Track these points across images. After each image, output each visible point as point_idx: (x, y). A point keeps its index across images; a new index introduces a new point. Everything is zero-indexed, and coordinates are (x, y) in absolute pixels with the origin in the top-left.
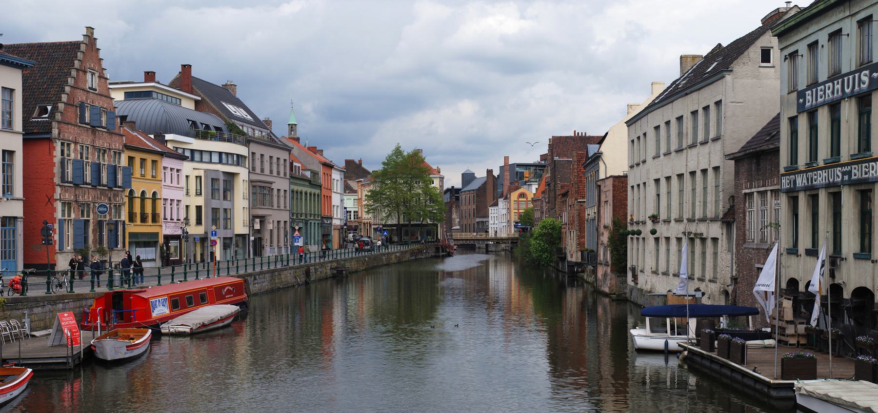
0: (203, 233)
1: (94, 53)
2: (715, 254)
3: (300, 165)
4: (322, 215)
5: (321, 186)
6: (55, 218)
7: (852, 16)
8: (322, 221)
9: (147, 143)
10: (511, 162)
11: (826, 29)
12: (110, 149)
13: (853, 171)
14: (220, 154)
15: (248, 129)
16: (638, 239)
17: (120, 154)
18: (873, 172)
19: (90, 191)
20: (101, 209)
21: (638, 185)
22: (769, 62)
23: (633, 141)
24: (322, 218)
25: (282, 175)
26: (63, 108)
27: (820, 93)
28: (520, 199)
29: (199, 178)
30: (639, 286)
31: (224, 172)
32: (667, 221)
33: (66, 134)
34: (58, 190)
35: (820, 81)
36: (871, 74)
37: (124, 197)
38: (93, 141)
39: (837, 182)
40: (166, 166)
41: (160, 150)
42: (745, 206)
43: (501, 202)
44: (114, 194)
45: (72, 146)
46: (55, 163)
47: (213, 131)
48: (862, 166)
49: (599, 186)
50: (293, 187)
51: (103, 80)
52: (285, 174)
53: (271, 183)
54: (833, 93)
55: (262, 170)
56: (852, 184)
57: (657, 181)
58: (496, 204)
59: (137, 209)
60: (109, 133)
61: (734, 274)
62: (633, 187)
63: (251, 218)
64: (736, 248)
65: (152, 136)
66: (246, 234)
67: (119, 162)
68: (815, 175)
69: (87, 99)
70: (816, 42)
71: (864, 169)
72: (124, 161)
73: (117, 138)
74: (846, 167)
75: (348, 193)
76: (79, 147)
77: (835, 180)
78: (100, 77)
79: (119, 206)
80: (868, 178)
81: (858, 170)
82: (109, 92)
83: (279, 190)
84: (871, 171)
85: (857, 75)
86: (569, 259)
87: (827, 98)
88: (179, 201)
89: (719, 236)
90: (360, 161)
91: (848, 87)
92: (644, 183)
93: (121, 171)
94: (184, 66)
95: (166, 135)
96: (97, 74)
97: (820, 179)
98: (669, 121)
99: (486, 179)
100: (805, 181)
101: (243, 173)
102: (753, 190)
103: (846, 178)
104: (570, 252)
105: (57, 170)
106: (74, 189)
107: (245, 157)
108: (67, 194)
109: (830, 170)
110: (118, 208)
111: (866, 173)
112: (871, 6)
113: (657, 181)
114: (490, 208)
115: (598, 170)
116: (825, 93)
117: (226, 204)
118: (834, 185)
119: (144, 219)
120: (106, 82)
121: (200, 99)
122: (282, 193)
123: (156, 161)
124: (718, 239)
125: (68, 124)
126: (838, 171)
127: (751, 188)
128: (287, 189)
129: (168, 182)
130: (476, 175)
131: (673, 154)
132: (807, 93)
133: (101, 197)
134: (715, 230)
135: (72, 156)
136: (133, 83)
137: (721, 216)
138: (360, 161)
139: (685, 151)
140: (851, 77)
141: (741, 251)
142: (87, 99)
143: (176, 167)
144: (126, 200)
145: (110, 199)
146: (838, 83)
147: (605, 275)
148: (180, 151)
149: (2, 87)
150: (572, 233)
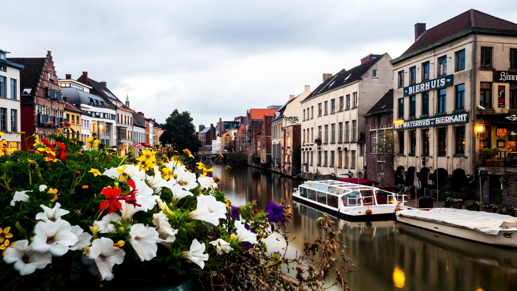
1: (51, 64)
2: (353, 158)
7: (435, 56)
10: (222, 121)
11: (421, 61)
12: (59, 110)
13: (436, 120)
14: (104, 114)
16: (308, 152)
17: (63, 112)
18: (448, 120)
21: (308, 129)
22: (376, 76)
23: (304, 110)
25: (130, 124)
27: (417, 88)
28: (227, 137)
30: (309, 172)
32: (326, 144)
34: (37, 129)
35: (417, 83)
36: (446, 80)
38: (51, 106)
39: (428, 125)
42: (371, 136)
43: (218, 138)
45: (43, 108)
47: (100, 103)
48: (441, 118)
49: (285, 130)
51: (55, 77)
52: (131, 124)
53: (126, 128)
54: (425, 88)
55: (122, 122)
56: (435, 125)
57: (320, 127)
58: (216, 139)
61: (365, 165)
62: (304, 130)
64: (366, 154)
65: (74, 105)
68: (414, 122)
69: (48, 86)
70: (415, 67)
71: (442, 120)
72: (65, 117)
73: (61, 105)
74: (456, 116)
76: (45, 109)
77: (426, 124)
80: (445, 123)
81: (439, 120)
82: (58, 82)
83: (129, 131)
84: (446, 120)
85: (438, 80)
86: (262, 162)
87: (421, 90)
89: (356, 150)
90: (154, 119)
91: (433, 85)
92: (312, 128)
94: (84, 73)
96: (53, 74)
97: (418, 124)
98: (327, 101)
99: (210, 128)
100: (408, 125)
102: (375, 130)
103: (432, 123)
104: (262, 159)
105: (36, 119)
107: (114, 116)
109: (423, 120)
111: (443, 121)
112: (446, 51)
113: (320, 127)
114: (213, 141)
115: (282, 123)
116: (420, 88)
117: (107, 138)
118: (425, 126)
120: (57, 78)
121: (92, 88)
124: (355, 151)
125: (40, 97)
126: (428, 120)
127: (375, 128)
130: (205, 126)
131: (329, 115)
132: (410, 88)
134: (354, 147)
135: (43, 113)
137: (357, 140)
138: (154, 119)
139: (336, 114)
140: (435, 81)
141: (369, 156)
142: (48, 86)
143: (87, 120)
146: (428, 84)
147: (289, 167)
148: (89, 113)
149: (11, 78)
150: (263, 151)
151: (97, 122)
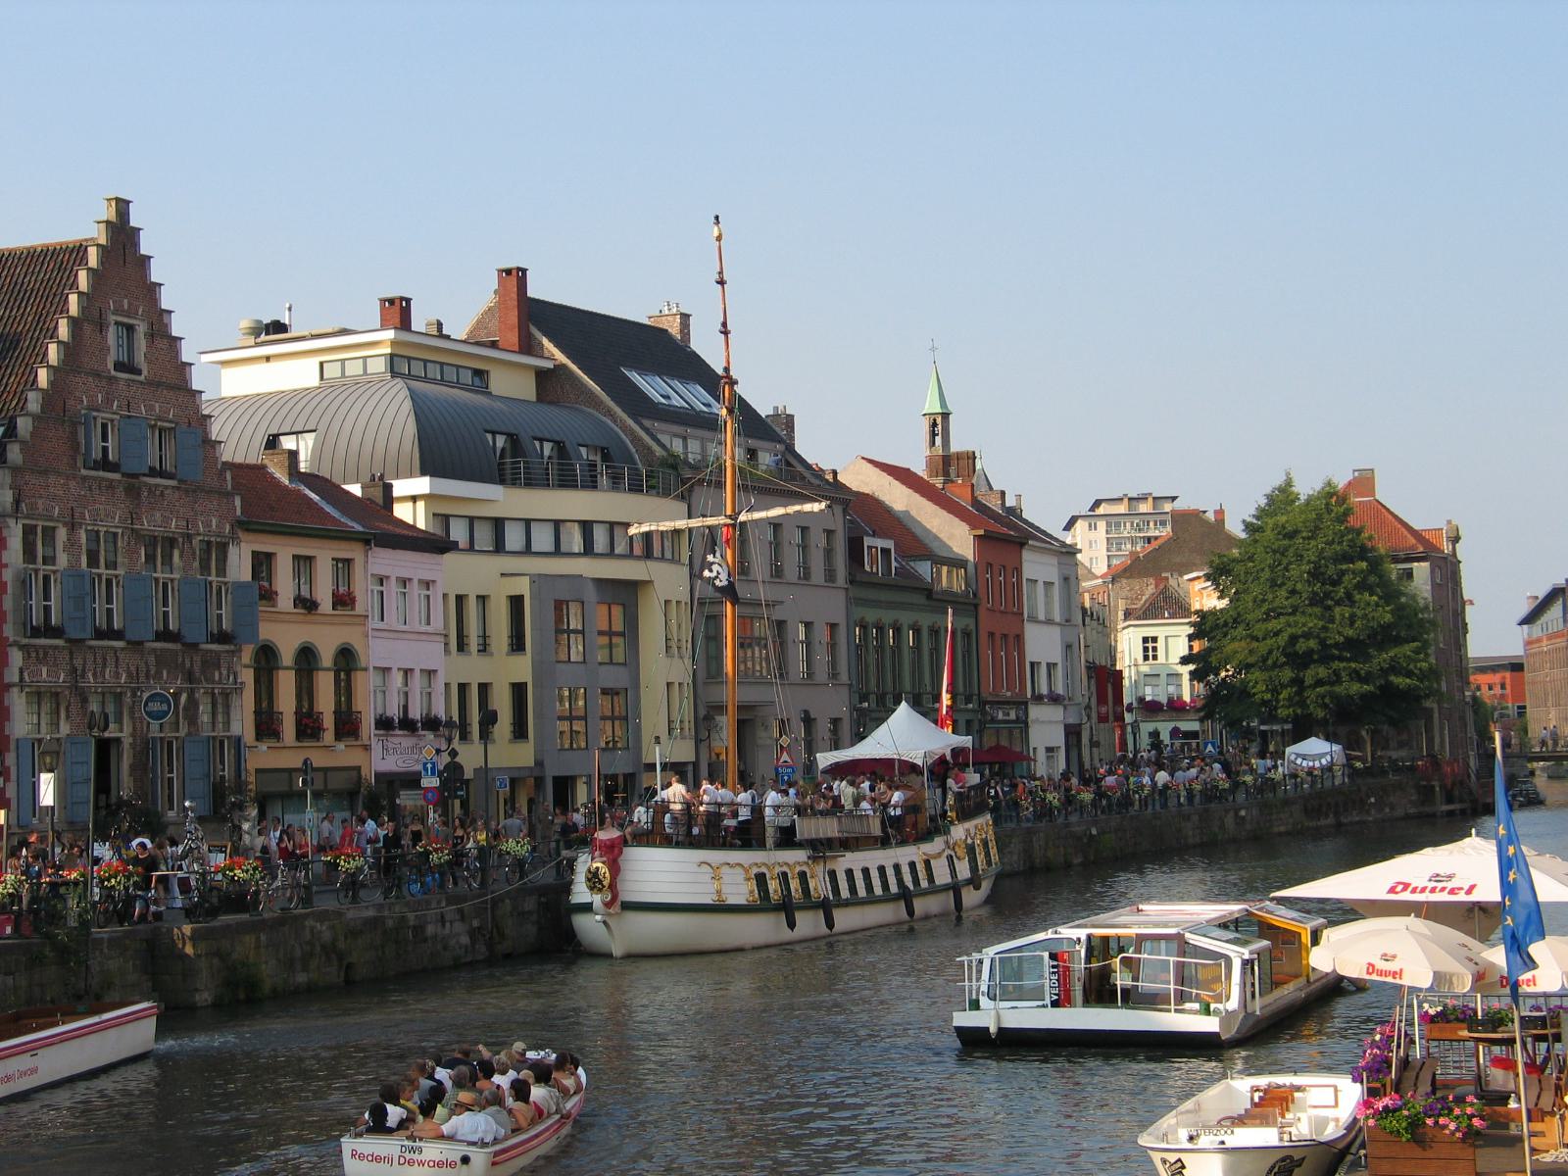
0: (532, 764)
3: (889, 544)
4: (983, 695)
5: (976, 606)
6: (8, 736)
8: (984, 713)
9: (328, 508)
14: (587, 527)
15: (685, 447)
17: (223, 549)
19: (121, 656)
20: (155, 707)
24: (983, 703)
25: (818, 574)
26: (30, 428)
29: (516, 602)
31: (601, 583)
33: (40, 502)
34: (16, 658)
37: (238, 669)
38: (134, 516)
40: (406, 576)
41: (361, 529)
44: (204, 663)
45: (62, 534)
46: (6, 583)
50: (860, 612)
52: (830, 575)
59: (286, 701)
60: (187, 491)
63: (702, 712)
66: (685, 764)
67: (222, 570)
69: (108, 401)
72: (239, 565)
75: (1171, 617)
78: (151, 336)
79: (226, 695)
88: (430, 673)
90: (1220, 513)
93: (229, 596)
95: (394, 482)
96: (142, 328)
101: (668, 582)
105: (8, 603)
106: (66, 652)
108: (44, 670)
110: (223, 701)
119: (309, 728)
122: (822, 635)
123: (348, 562)
125: (45, 472)
128: (840, 618)
129: (392, 620)
133: (159, 674)
135: (62, 560)
136: (344, 332)
138: (1220, 513)
142: (108, 401)
144: (247, 677)
145: (190, 677)
151: (526, 580)
